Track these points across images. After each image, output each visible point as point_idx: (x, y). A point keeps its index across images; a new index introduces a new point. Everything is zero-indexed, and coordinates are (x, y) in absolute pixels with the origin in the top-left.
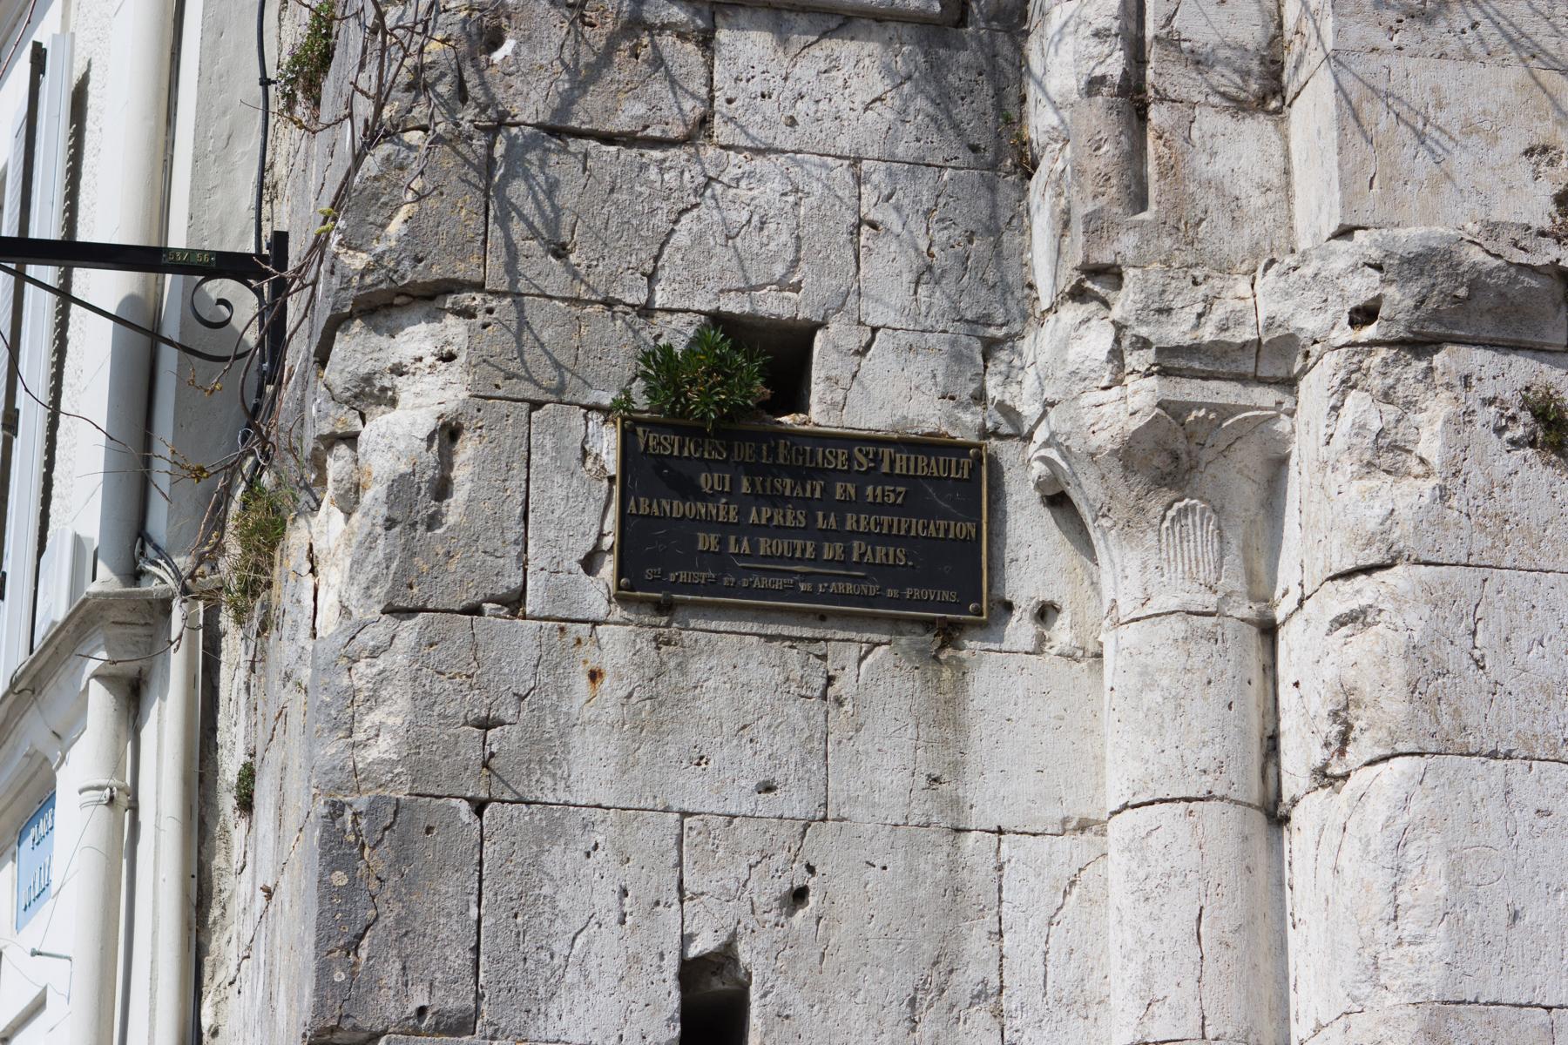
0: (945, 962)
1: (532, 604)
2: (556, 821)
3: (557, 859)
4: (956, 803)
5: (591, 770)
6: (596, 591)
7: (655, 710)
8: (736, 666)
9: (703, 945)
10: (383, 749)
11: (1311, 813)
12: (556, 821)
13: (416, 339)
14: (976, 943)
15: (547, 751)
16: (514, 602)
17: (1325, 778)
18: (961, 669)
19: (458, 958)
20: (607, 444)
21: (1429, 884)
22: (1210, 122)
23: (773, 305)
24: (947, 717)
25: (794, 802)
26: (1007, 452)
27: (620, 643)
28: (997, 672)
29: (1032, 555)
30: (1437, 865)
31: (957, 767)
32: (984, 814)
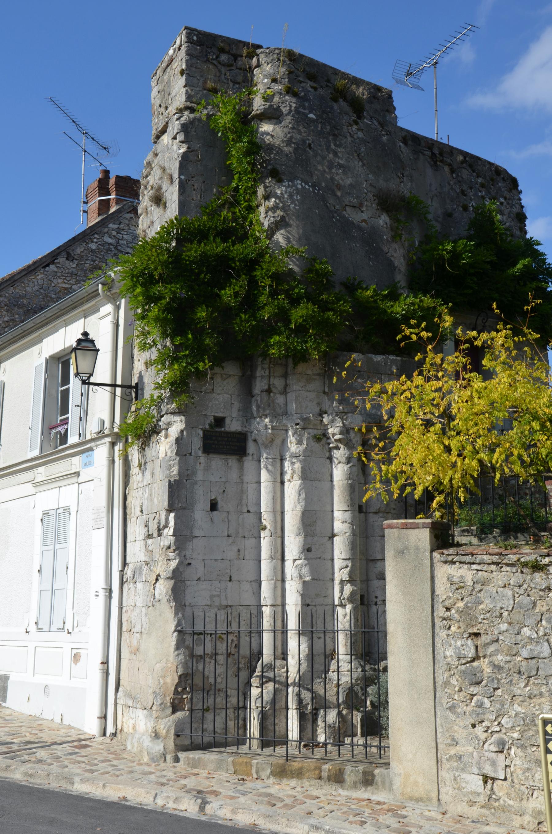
0: (241, 499)
1: (193, 454)
2: (196, 483)
3: (196, 487)
4: (242, 479)
5: (200, 476)
6: (200, 453)
7: (207, 469)
8: (217, 461)
9: (213, 498)
10: (175, 473)
11: (286, 484)
12: (196, 483)
13: (178, 418)
14: (245, 497)
15: (194, 473)
16: (190, 454)
17: (289, 480)
18: (243, 462)
19: (184, 500)
20: (201, 433)
21: (303, 496)
22: (277, 395)
23: (220, 415)
24: (241, 468)
25: (223, 480)
26: (249, 434)
27: (203, 459)
28: (248, 463)
29: (251, 448)
30: (304, 494)
31: (242, 475)
32: (246, 480)
